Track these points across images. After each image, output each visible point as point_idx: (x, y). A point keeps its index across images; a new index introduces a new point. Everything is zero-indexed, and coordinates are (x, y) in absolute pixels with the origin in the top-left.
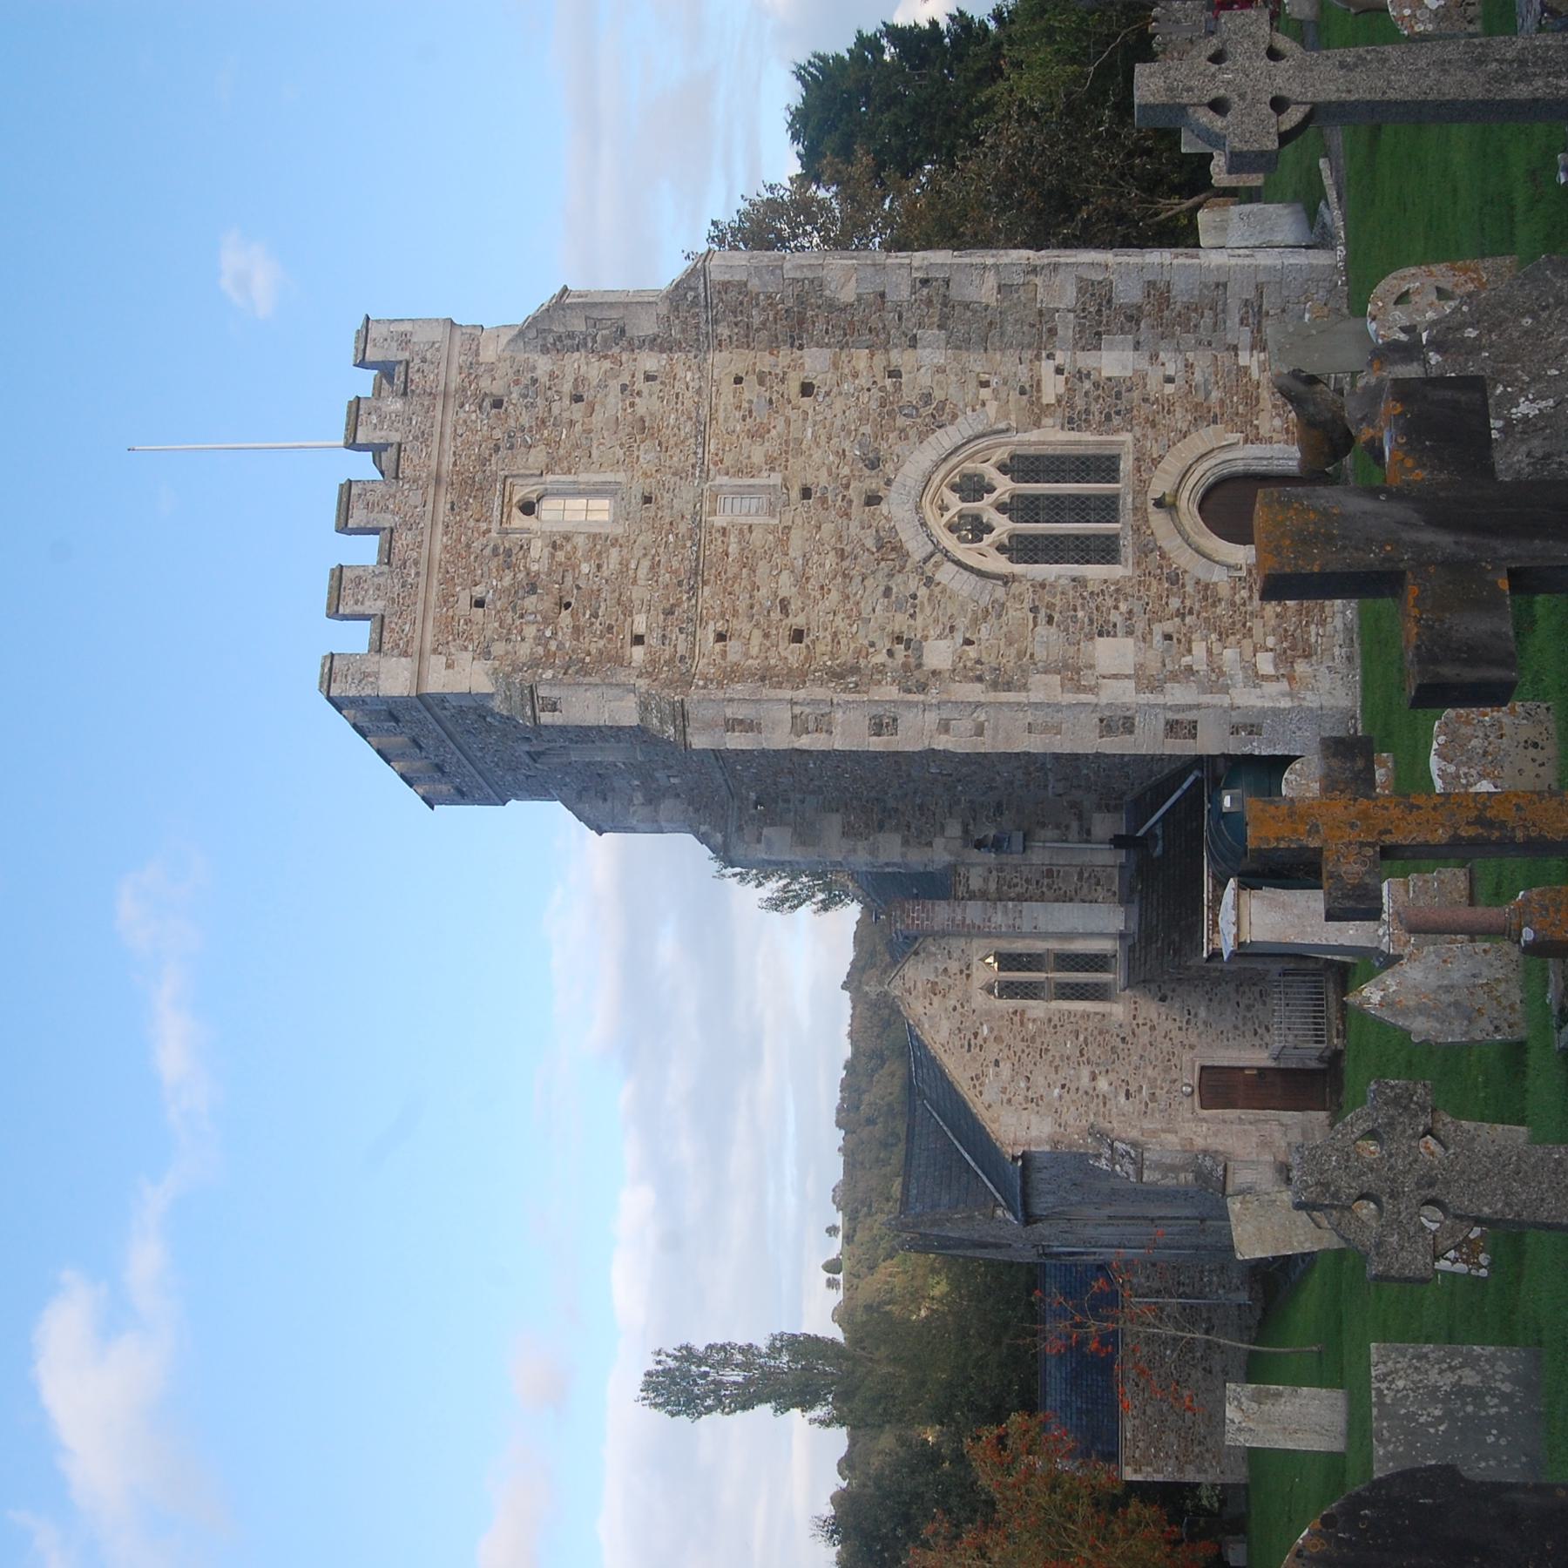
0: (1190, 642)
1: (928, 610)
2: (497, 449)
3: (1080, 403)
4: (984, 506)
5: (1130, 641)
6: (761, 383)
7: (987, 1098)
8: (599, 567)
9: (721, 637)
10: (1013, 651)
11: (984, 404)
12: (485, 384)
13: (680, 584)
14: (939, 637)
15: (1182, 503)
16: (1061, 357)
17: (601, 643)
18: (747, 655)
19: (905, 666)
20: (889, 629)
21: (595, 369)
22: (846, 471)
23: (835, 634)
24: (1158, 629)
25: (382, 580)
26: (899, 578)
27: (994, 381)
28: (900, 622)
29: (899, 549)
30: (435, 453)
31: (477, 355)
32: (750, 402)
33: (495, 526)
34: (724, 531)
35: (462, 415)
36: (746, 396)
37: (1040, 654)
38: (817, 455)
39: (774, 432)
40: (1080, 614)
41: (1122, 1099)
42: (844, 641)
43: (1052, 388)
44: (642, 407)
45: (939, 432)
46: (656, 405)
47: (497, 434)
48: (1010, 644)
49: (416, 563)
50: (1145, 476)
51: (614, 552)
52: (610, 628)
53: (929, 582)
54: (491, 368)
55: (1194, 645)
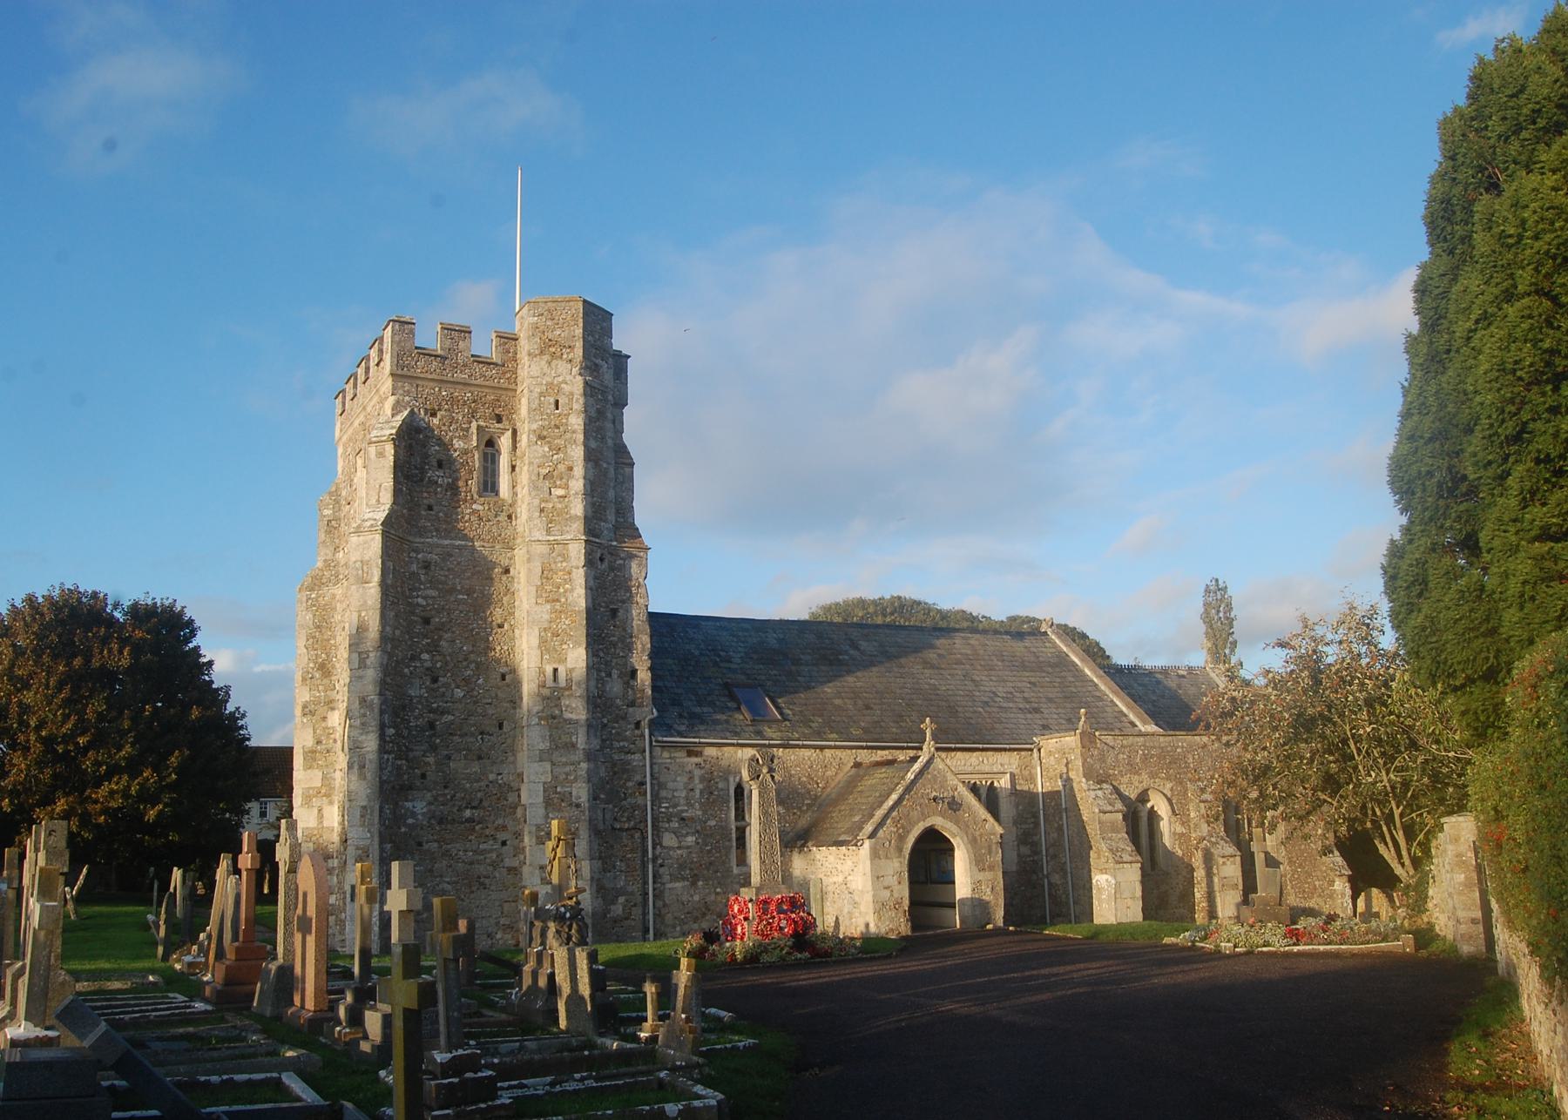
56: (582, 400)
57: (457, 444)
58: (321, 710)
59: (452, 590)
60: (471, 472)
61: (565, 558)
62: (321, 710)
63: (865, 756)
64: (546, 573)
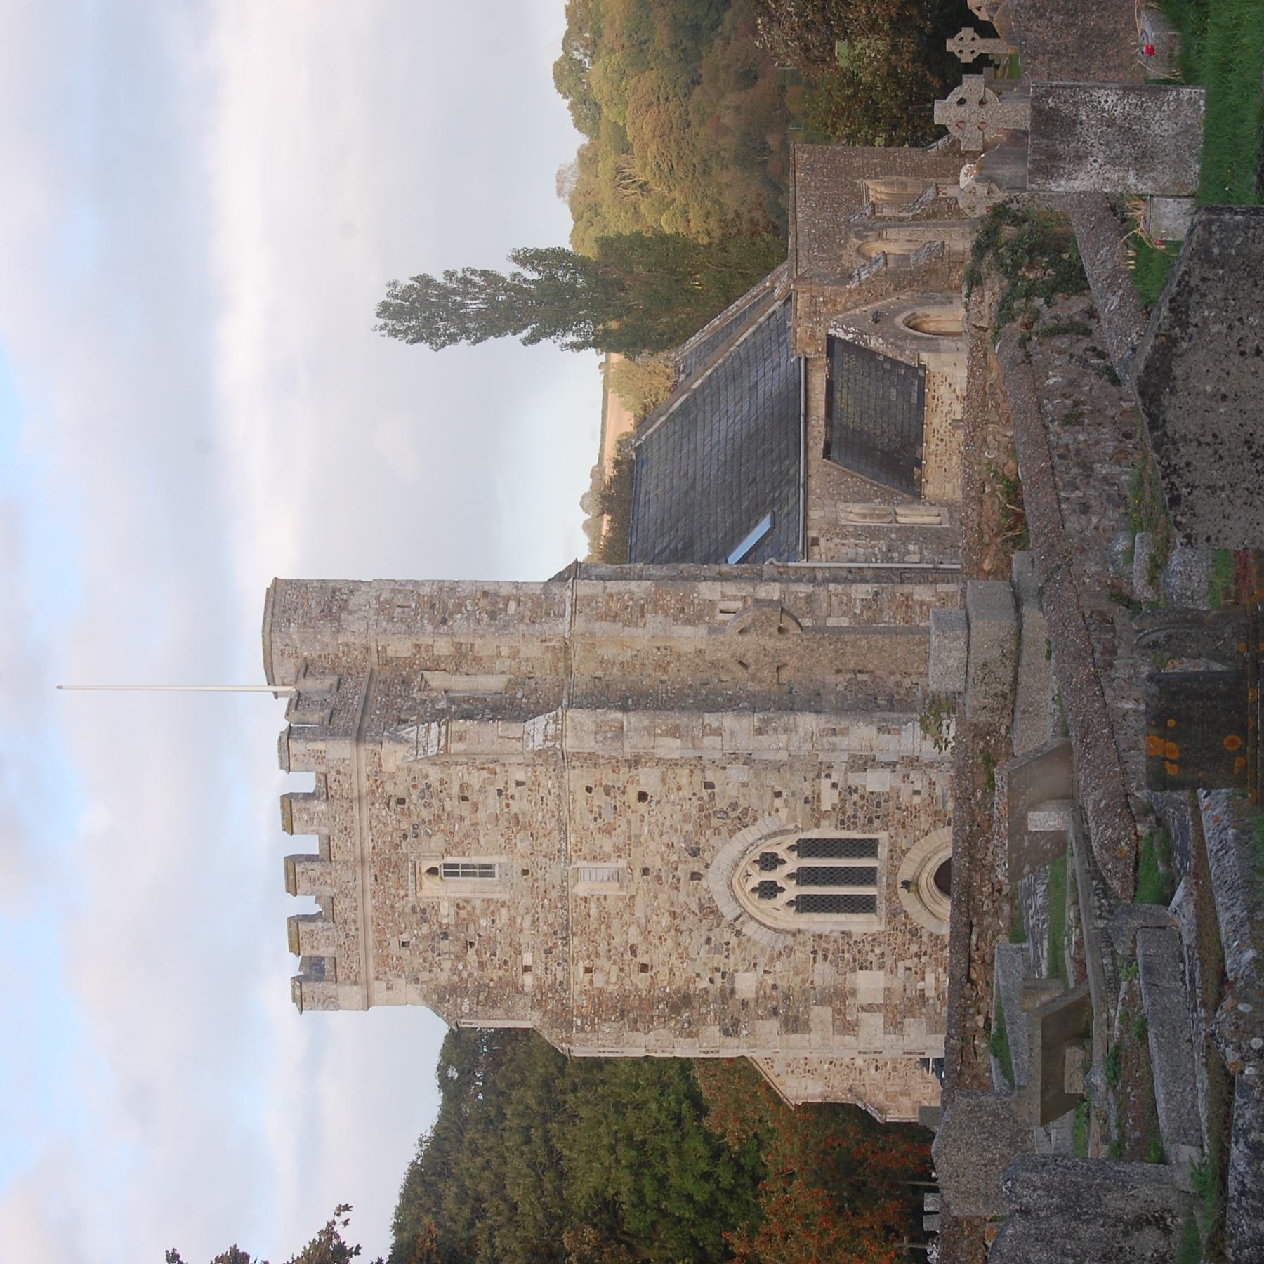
0: (924, 973)
1: (738, 951)
2: (405, 837)
3: (850, 812)
4: (778, 875)
5: (882, 973)
6: (607, 794)
7: (776, 1070)
8: (493, 921)
9: (588, 970)
10: (799, 979)
11: (777, 811)
12: (389, 788)
13: (555, 933)
14: (746, 971)
15: (923, 883)
16: (835, 778)
17: (501, 973)
18: (607, 982)
19: (722, 990)
20: (710, 965)
21: (476, 779)
22: (675, 858)
23: (671, 970)
24: (900, 964)
25: (329, 933)
26: (717, 931)
27: (785, 794)
28: (718, 960)
29: (715, 912)
30: (358, 843)
31: (380, 765)
32: (599, 807)
34: (586, 900)
35: (373, 810)
36: (596, 802)
37: (818, 982)
38: (652, 846)
39: (619, 830)
40: (847, 955)
41: (873, 1070)
42: (677, 974)
43: (829, 799)
44: (515, 807)
45: (744, 831)
46: (526, 806)
47: (405, 825)
48: (796, 974)
49: (354, 922)
50: (896, 863)
51: (504, 911)
52: (506, 963)
53: (738, 933)
54: (392, 776)
55: (926, 976)
58: (733, 1006)
61: (593, 598)
64: (608, 616)
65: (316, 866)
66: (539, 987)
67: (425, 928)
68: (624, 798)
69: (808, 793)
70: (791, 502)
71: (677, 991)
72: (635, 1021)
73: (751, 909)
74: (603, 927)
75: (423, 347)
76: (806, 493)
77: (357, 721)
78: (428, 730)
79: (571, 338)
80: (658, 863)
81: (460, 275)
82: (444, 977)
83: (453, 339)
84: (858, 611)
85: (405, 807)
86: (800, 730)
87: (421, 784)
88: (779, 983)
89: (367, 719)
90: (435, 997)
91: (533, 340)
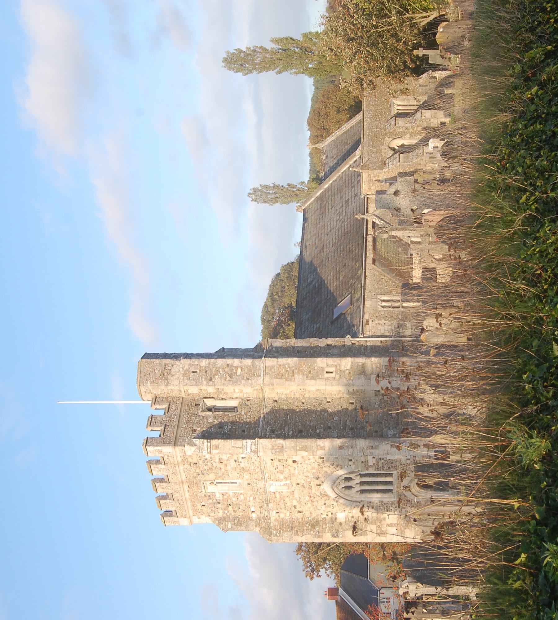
1: (337, 507)
3: (380, 465)
12: (190, 460)
19: (331, 518)
22: (309, 480)
27: (353, 461)
28: (330, 509)
29: (327, 496)
33: (203, 491)
43: (371, 461)
44: (242, 465)
46: (247, 465)
47: (198, 471)
51: (242, 496)
54: (190, 456)
56: (194, 360)
57: (211, 420)
58: (336, 526)
59: (286, 421)
60: (225, 415)
61: (272, 367)
62: (336, 526)
63: (370, 255)
64: (280, 376)
65: (164, 484)
66: (259, 518)
67: (211, 501)
68: (287, 463)
69: (363, 460)
70: (359, 293)
71: (314, 519)
72: (297, 532)
73: (341, 495)
74: (282, 501)
75: (240, 74)
76: (364, 290)
77: (175, 434)
78: (203, 443)
79: (294, 70)
80: (303, 482)
81: (252, 49)
82: (220, 515)
83: (251, 71)
84: (384, 371)
85: (197, 465)
86: (358, 447)
87: (203, 459)
88: (354, 515)
89: (179, 431)
90: (217, 522)
91: (279, 72)
